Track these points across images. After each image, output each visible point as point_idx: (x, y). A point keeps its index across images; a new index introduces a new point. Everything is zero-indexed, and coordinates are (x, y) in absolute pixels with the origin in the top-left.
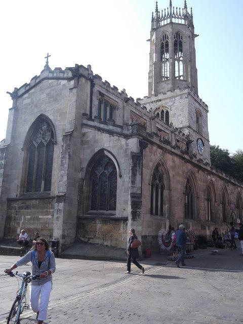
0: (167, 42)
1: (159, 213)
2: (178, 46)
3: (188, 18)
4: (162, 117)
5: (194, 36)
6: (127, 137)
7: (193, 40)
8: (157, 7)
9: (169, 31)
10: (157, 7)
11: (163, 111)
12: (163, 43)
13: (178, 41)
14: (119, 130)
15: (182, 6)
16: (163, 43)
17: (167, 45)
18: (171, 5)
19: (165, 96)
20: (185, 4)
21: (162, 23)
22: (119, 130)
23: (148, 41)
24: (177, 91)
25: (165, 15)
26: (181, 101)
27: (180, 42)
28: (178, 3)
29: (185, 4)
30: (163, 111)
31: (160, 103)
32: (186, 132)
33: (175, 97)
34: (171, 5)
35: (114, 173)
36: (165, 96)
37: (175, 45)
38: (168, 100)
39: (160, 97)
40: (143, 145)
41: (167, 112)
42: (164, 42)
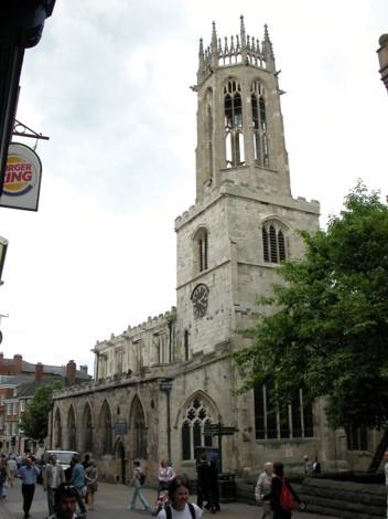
0: (237, 95)
8: (214, 32)
10: (214, 32)
12: (228, 97)
13: (258, 96)
15: (262, 39)
16: (228, 97)
17: (238, 101)
18: (243, 32)
20: (267, 34)
21: (221, 62)
23: (194, 89)
25: (232, 48)
29: (267, 34)
34: (243, 32)
37: (254, 102)
42: (232, 95)
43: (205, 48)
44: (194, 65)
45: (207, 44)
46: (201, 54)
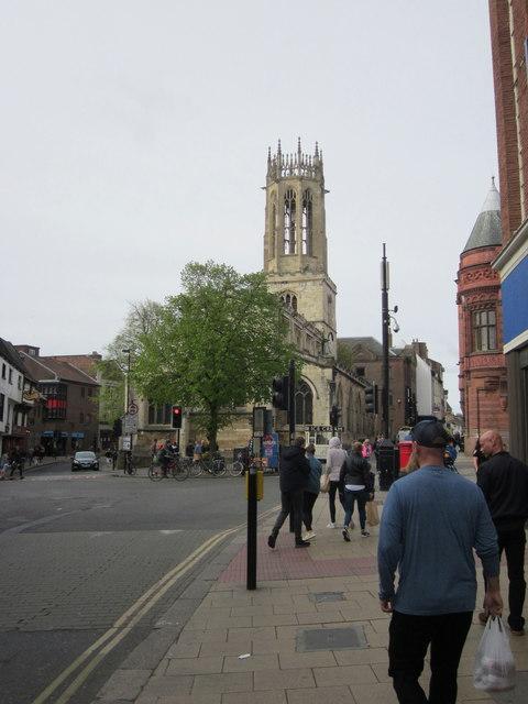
1: (164, 418)
2: (308, 204)
3: (319, 167)
4: (288, 301)
5: (324, 192)
6: (323, 367)
7: (323, 197)
9: (298, 189)
11: (288, 296)
14: (314, 360)
18: (299, 152)
19: (292, 278)
22: (314, 360)
24: (309, 275)
26: (314, 288)
27: (310, 203)
28: (308, 151)
30: (288, 296)
31: (285, 286)
32: (320, 327)
33: (306, 281)
34: (299, 152)
35: (310, 397)
36: (292, 278)
38: (297, 284)
39: (287, 278)
40: (334, 374)
41: (295, 298)
43: (272, 158)
44: (263, 170)
45: (274, 152)
46: (269, 160)
